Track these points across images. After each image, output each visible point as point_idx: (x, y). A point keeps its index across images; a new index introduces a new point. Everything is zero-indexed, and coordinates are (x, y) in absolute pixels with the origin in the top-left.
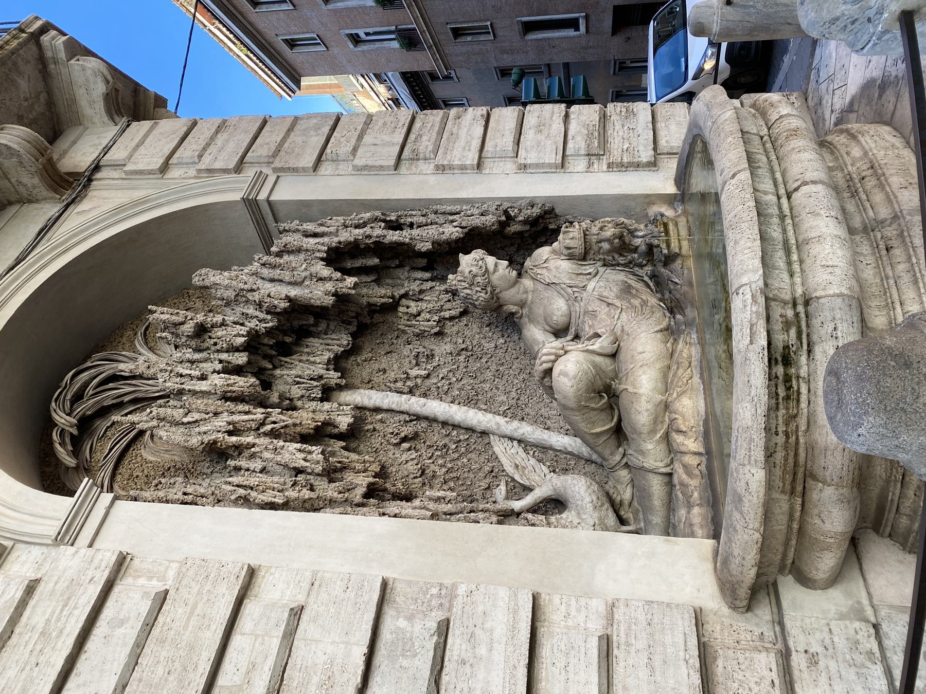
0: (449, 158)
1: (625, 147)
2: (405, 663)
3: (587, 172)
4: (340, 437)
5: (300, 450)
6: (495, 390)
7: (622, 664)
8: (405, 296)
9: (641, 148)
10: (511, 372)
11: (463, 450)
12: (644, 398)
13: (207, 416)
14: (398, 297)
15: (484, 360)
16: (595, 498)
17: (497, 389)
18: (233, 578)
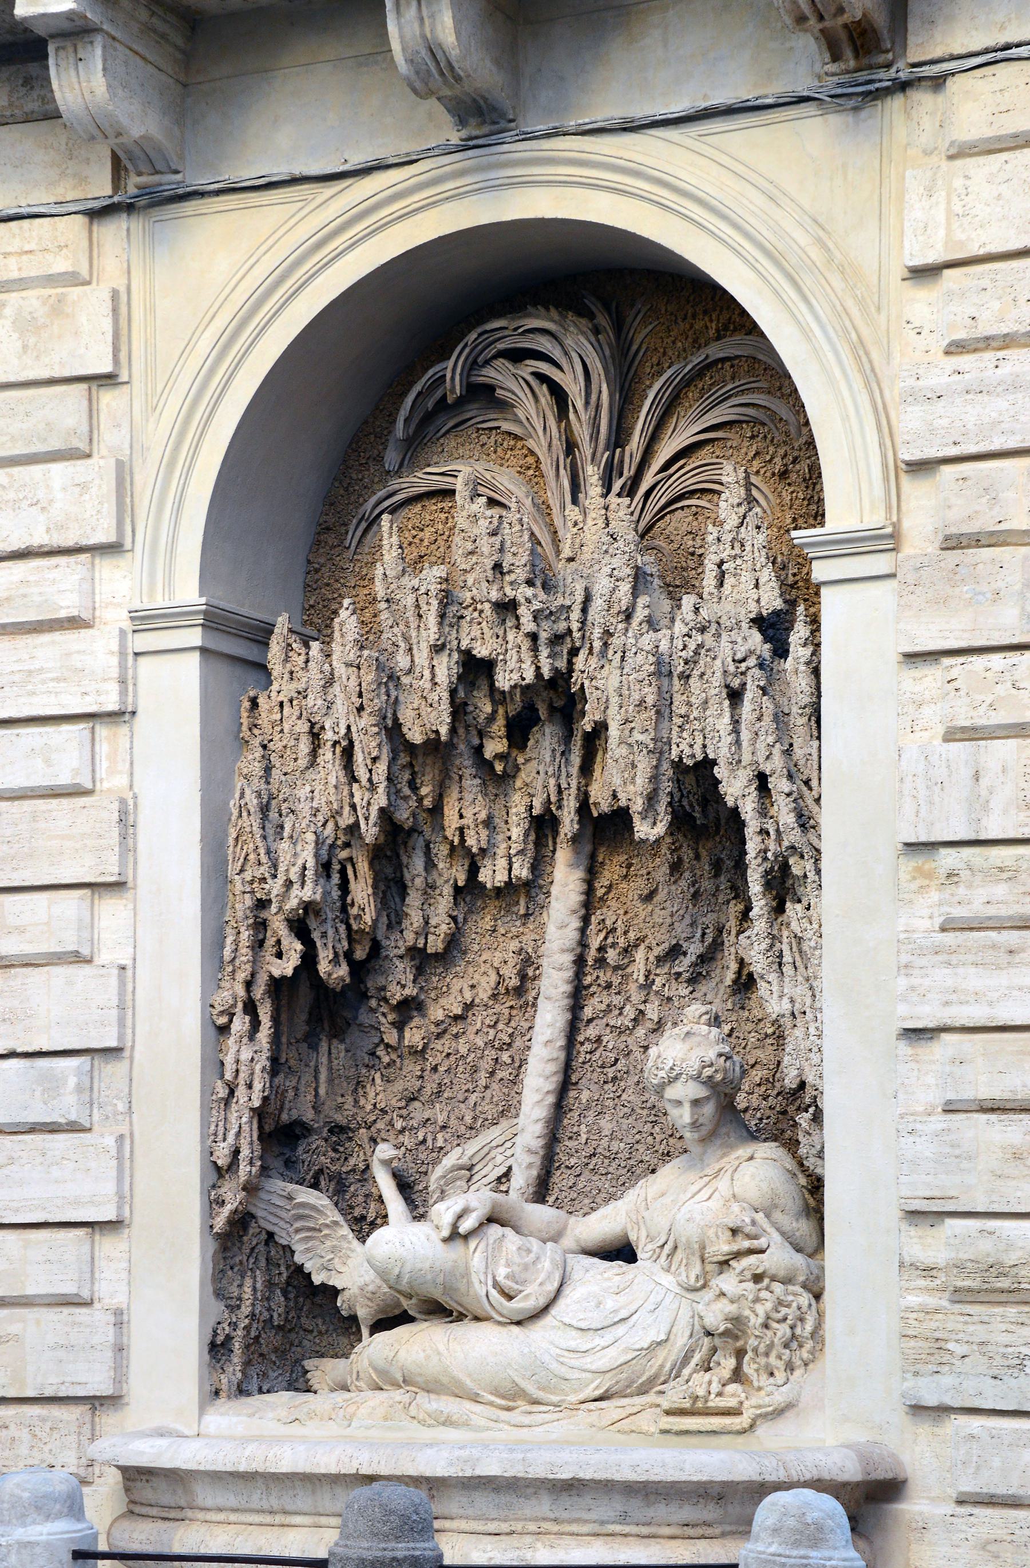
0: (923, 961)
1: (950, 1346)
2: (38, 1093)
3: (901, 1265)
4: (473, 870)
5: (305, 868)
7: (56, 1318)
9: (947, 1380)
10: (658, 1138)
16: (371, 1288)
18: (101, 869)
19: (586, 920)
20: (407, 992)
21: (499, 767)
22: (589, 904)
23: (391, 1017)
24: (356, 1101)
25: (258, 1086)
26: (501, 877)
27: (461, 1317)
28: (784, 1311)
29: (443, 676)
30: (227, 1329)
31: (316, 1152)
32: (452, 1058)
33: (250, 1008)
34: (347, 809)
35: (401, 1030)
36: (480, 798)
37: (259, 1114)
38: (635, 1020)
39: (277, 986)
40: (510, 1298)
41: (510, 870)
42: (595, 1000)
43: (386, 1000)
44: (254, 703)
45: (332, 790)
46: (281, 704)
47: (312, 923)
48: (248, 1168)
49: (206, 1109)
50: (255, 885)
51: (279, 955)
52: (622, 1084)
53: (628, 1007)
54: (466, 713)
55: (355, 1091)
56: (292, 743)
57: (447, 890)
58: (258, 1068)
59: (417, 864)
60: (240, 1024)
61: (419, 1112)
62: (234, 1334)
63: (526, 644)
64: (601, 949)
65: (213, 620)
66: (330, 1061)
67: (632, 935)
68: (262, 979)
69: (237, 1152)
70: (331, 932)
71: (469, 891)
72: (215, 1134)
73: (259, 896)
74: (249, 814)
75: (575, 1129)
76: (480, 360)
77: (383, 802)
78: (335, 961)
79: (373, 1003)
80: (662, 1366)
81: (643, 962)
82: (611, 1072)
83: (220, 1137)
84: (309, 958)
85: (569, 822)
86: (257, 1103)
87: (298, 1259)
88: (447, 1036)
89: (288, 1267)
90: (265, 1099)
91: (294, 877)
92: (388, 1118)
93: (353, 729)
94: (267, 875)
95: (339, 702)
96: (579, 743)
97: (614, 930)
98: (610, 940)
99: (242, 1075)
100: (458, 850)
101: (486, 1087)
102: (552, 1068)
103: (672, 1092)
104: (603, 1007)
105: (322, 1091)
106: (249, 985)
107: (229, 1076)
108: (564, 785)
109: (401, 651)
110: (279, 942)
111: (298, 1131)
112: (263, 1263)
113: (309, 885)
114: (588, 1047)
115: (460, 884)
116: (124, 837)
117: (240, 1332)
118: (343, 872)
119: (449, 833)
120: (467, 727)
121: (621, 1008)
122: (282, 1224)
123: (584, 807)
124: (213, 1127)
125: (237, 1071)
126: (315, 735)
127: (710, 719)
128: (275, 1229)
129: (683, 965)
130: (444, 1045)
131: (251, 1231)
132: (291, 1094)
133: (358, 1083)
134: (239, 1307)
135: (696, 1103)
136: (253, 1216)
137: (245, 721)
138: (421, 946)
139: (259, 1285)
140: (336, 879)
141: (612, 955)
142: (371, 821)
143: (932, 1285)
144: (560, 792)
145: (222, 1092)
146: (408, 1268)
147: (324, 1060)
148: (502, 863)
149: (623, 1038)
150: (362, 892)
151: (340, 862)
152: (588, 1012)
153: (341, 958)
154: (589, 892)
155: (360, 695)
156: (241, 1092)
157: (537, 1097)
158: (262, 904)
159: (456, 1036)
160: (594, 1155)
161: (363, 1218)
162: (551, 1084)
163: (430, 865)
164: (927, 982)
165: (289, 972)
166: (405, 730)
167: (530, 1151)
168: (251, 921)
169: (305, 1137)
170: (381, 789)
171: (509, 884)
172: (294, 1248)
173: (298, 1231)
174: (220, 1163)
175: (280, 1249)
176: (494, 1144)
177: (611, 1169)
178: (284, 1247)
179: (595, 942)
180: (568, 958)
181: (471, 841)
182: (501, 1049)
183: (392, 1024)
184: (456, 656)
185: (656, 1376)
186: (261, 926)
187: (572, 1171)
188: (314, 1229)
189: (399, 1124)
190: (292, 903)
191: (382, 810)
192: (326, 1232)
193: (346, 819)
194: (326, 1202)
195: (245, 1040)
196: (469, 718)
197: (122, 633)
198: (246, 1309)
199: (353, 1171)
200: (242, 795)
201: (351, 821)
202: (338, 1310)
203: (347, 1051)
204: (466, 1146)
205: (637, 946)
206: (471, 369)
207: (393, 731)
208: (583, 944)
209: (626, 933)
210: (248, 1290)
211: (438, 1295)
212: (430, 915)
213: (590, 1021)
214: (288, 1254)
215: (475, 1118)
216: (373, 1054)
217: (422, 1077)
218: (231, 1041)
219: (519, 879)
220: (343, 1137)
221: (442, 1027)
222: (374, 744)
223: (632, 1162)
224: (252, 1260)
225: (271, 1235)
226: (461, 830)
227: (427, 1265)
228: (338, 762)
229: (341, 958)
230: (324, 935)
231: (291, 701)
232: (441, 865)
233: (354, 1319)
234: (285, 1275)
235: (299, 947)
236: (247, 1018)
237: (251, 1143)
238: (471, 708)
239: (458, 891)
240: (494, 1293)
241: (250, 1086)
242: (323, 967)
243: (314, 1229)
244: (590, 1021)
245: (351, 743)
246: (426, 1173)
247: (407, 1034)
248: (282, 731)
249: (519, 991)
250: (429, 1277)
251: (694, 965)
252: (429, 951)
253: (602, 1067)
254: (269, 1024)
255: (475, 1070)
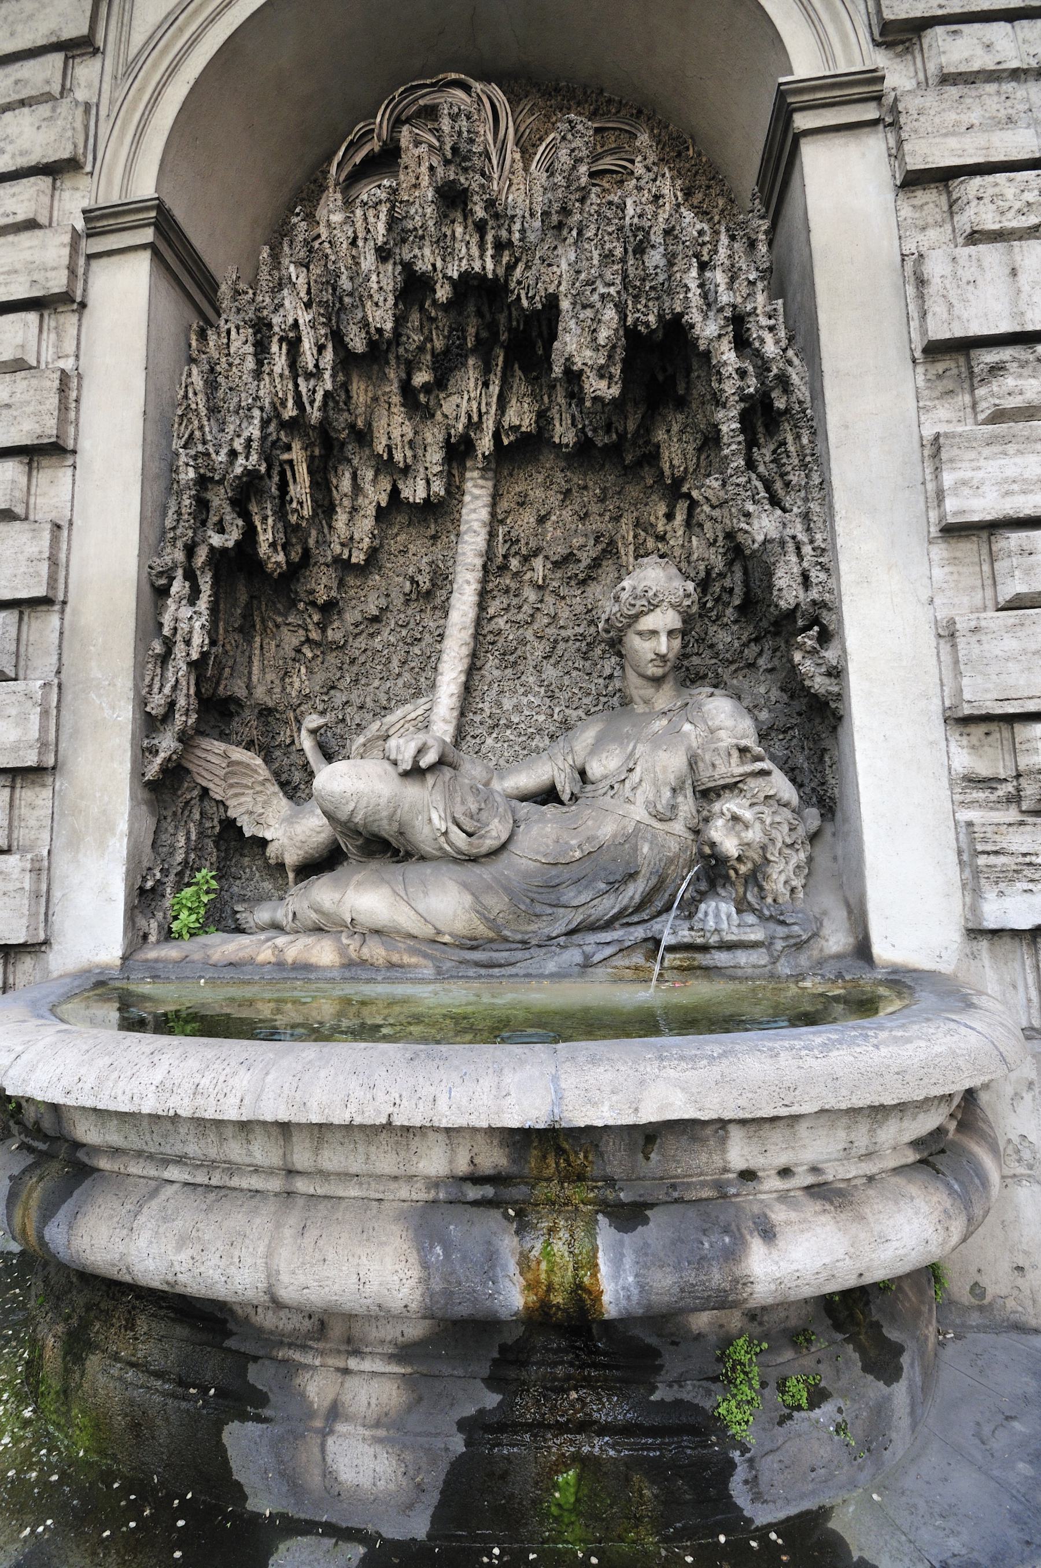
4: (395, 492)
6: (522, 690)
8: (693, 504)
11: (413, 664)
12: (337, 896)
13: (303, 294)
14: (685, 489)
15: (580, 663)
17: (525, 694)
19: (492, 535)
20: (333, 594)
21: (422, 398)
22: (495, 521)
23: (316, 618)
24: (284, 689)
25: (197, 640)
26: (421, 494)
27: (408, 856)
28: (794, 836)
29: (388, 284)
30: (158, 876)
31: (248, 724)
32: (369, 653)
33: (190, 576)
34: (290, 403)
35: (324, 630)
36: (407, 423)
37: (197, 666)
38: (532, 615)
39: (217, 556)
40: (470, 835)
41: (429, 490)
42: (497, 602)
43: (313, 604)
44: (202, 335)
45: (278, 380)
46: (229, 332)
47: (254, 508)
48: (184, 718)
49: (139, 667)
50: (200, 461)
51: (221, 530)
52: (521, 667)
53: (525, 608)
54: (398, 345)
55: (283, 679)
56: (237, 361)
57: (371, 511)
58: (197, 625)
59: (346, 484)
60: (179, 586)
61: (339, 698)
62: (166, 880)
63: (475, 240)
64: (505, 557)
65: (164, 221)
66: (262, 654)
67: (533, 544)
68: (202, 555)
69: (172, 705)
70: (270, 521)
71: (395, 506)
72: (150, 686)
73: (202, 471)
74: (195, 394)
75: (480, 706)
76: (403, 118)
77: (329, 386)
78: (273, 545)
79: (301, 606)
80: (632, 898)
81: (541, 569)
82: (512, 658)
83: (156, 690)
84: (250, 533)
85: (485, 444)
86: (195, 656)
87: (232, 813)
88: (364, 635)
89: (221, 822)
90: (204, 655)
91: (238, 445)
92: (311, 703)
93: (301, 321)
94: (211, 450)
95: (287, 303)
96: (499, 374)
97: (518, 541)
98: (512, 551)
99: (179, 632)
100: (385, 465)
101: (399, 675)
102: (465, 651)
103: (647, 622)
104: (505, 606)
105: (255, 679)
106: (190, 550)
107: (166, 631)
108: (484, 410)
109: (344, 277)
110: (221, 521)
111: (233, 708)
112: (197, 816)
113: (254, 457)
114: (490, 638)
115: (383, 504)
116: (63, 407)
117: (172, 877)
118: (282, 474)
119: (380, 449)
120: (398, 357)
121: (520, 607)
122: (217, 780)
123: (497, 436)
124: (148, 679)
125: (175, 629)
126: (261, 328)
127: (678, 275)
128: (211, 786)
129: (578, 569)
130: (361, 642)
131: (186, 785)
132: (227, 670)
133: (286, 673)
134: (171, 854)
135: (670, 633)
136: (188, 771)
137: (194, 343)
138: (345, 557)
139: (193, 837)
140: (276, 479)
141: (514, 563)
142: (317, 404)
143: (993, 797)
144: (480, 416)
145: (158, 647)
146: (363, 803)
147: (257, 652)
148: (421, 484)
149: (521, 631)
150: (301, 489)
151: (281, 465)
152: (491, 611)
153: (279, 548)
154: (493, 514)
155: (309, 292)
156: (179, 650)
157: (454, 675)
158: (203, 482)
159: (372, 635)
160: (497, 725)
161: (288, 783)
162: (463, 665)
163: (357, 488)
164: (980, 474)
165: (230, 544)
166: (347, 339)
167: (445, 721)
168: (193, 492)
169: (238, 714)
170: (327, 375)
171: (427, 500)
172: (228, 803)
173: (231, 786)
174: (154, 712)
175: (213, 804)
176: (409, 718)
177: (512, 737)
178: (217, 802)
179: (501, 550)
180: (479, 562)
181: (398, 456)
182: (412, 644)
183: (318, 624)
184: (399, 268)
185: (625, 909)
186: (202, 505)
187: (478, 740)
188: (247, 787)
189: (320, 707)
190: (238, 470)
191: (327, 395)
192: (258, 788)
193: (290, 411)
194: (259, 761)
195: (184, 602)
196: (401, 350)
197: (75, 235)
198: (179, 857)
199: (280, 745)
200: (189, 375)
201: (295, 413)
202: (266, 859)
203: (278, 646)
204: (386, 720)
205: (535, 556)
206: (393, 127)
207: (337, 337)
208: (489, 555)
209: (527, 544)
210: (182, 842)
211: (387, 829)
212: (354, 529)
213: (492, 618)
214: (222, 810)
215: (389, 700)
216: (298, 651)
217: (341, 668)
218: (170, 601)
219: (437, 494)
220: (270, 719)
221: (362, 627)
222: (323, 332)
223: (532, 730)
224: (186, 813)
225: (205, 791)
226: (389, 448)
227: (383, 801)
228: (284, 357)
229: (279, 548)
230: (265, 518)
231: (238, 328)
232: (367, 486)
233: (281, 866)
234: (218, 829)
235: (240, 522)
236: (187, 584)
237: (188, 696)
238: (404, 339)
239: (382, 514)
240: (455, 829)
241: (188, 643)
242: (263, 549)
243: (247, 787)
244: (492, 618)
245: (299, 339)
246: (344, 747)
247: (330, 632)
248: (229, 355)
249: (429, 595)
250: (385, 814)
251: (589, 567)
252: (354, 560)
253: (504, 654)
254: (209, 593)
255: (389, 661)
